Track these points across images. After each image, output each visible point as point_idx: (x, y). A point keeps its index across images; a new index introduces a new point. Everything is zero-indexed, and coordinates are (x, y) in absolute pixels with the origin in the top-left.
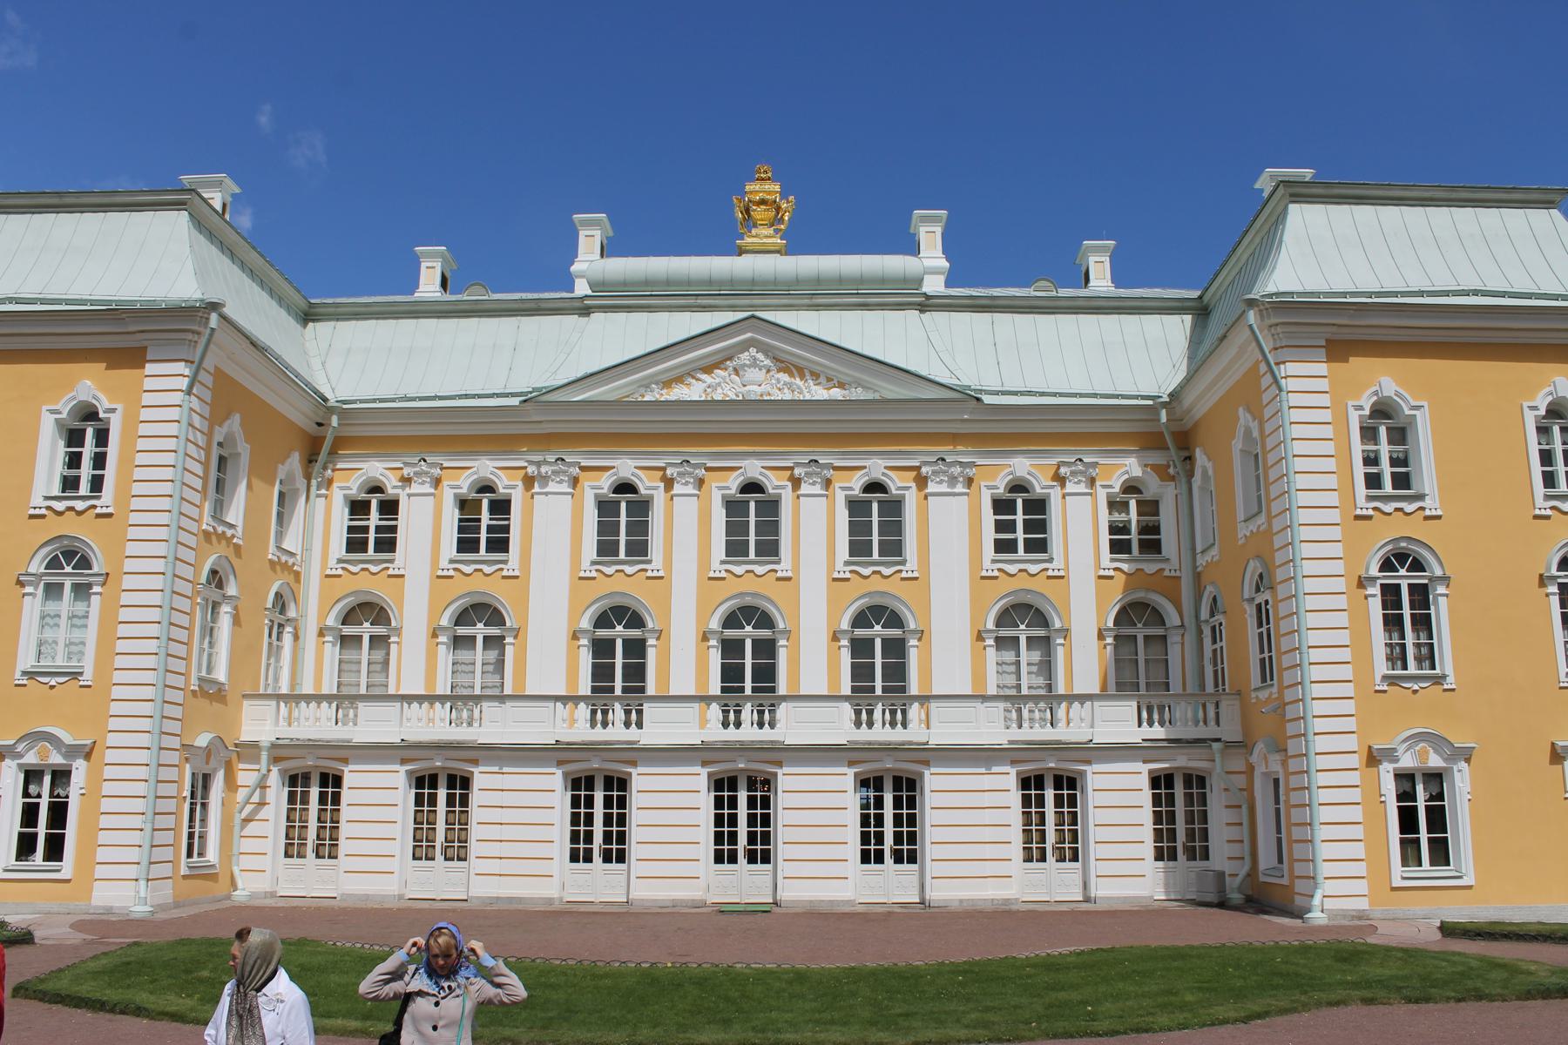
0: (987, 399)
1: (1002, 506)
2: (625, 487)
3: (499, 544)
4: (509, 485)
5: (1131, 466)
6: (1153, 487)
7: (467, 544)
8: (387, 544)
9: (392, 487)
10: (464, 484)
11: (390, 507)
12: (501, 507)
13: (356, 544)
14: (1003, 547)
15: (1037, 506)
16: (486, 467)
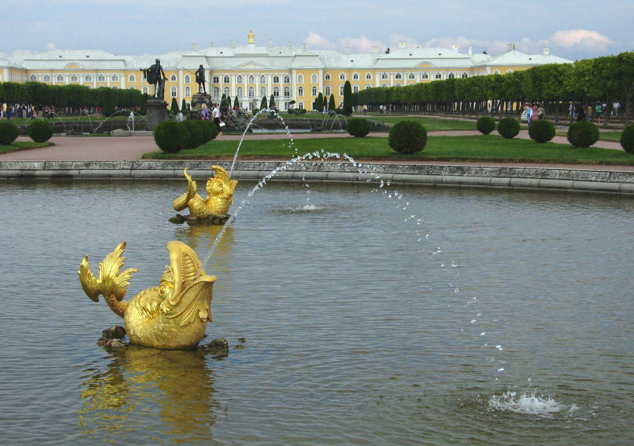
0: (273, 68)
1: (274, 78)
2: (240, 76)
3: (228, 82)
4: (228, 76)
5: (287, 74)
6: (288, 76)
7: (225, 81)
8: (218, 82)
9: (218, 76)
10: (225, 76)
11: (218, 78)
12: (228, 78)
13: (215, 82)
14: (274, 82)
15: (278, 78)
16: (226, 74)
